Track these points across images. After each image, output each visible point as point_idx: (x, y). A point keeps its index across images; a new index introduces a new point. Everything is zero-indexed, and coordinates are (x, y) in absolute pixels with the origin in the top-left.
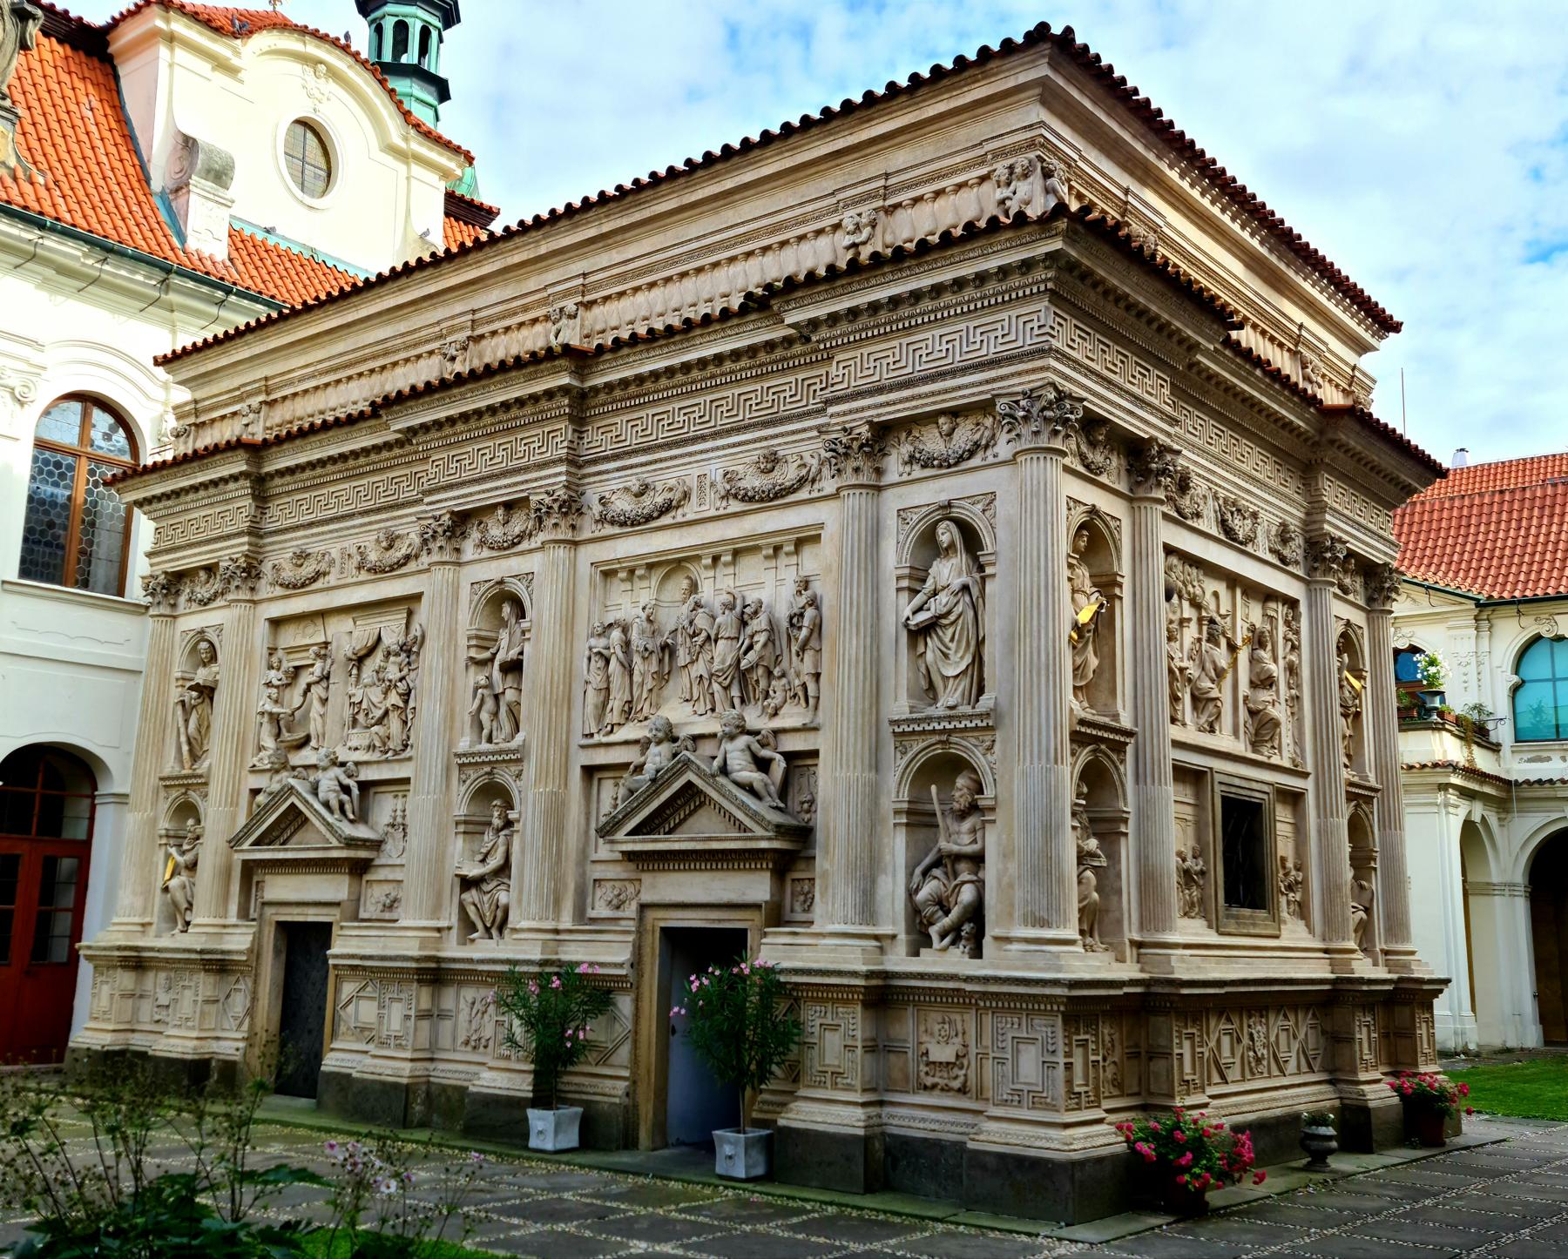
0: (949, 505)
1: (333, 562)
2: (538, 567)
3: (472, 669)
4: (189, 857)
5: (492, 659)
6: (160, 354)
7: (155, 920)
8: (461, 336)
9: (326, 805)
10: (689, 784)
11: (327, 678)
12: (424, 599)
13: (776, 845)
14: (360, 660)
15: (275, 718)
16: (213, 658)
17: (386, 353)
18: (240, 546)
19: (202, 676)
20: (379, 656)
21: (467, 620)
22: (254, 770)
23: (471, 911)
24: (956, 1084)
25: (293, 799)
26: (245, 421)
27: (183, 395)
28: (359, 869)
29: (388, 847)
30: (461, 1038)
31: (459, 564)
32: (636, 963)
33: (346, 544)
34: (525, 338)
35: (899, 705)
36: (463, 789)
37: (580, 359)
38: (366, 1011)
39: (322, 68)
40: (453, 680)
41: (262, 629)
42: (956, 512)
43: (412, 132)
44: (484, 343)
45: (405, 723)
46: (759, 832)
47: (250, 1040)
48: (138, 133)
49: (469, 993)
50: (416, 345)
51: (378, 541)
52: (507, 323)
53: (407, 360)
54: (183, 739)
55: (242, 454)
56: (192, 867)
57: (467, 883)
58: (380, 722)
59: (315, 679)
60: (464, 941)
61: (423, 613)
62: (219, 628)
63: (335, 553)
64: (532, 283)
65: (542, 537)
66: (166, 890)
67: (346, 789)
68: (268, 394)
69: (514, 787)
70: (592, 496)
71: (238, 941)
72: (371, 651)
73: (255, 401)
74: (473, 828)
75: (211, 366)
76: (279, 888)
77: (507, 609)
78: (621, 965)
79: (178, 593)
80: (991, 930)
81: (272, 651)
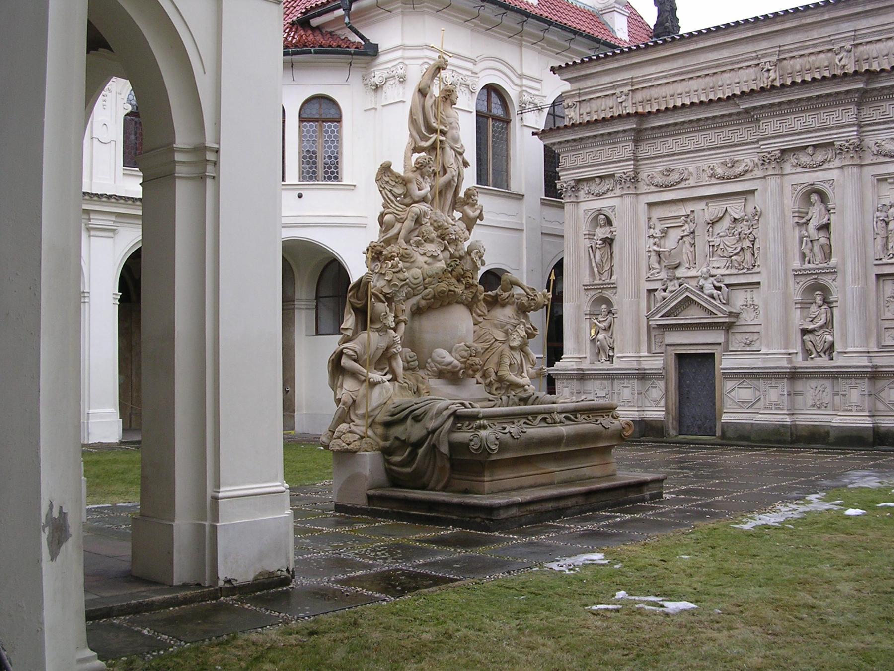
1: (691, 174)
2: (835, 177)
3: (797, 229)
4: (606, 324)
5: (807, 223)
6: (556, 64)
7: (588, 355)
8: (774, 59)
9: (712, 297)
11: (693, 232)
12: (756, 193)
14: (713, 223)
15: (658, 254)
16: (609, 222)
17: (718, 66)
18: (629, 166)
19: (602, 232)
20: (726, 223)
21: (791, 203)
22: (648, 280)
23: (809, 346)
25: (687, 294)
26: (620, 100)
27: (567, 87)
28: (728, 327)
29: (744, 315)
30: (810, 402)
31: (782, 175)
33: (699, 164)
36: (798, 287)
37: (871, 74)
38: (746, 394)
40: (784, 233)
41: (642, 207)
44: (785, 62)
45: (754, 255)
47: (667, 411)
49: (813, 383)
51: (724, 164)
52: (802, 52)
53: (731, 70)
54: (594, 265)
55: (635, 120)
56: (608, 328)
57: (805, 332)
58: (736, 255)
59: (686, 233)
60: (805, 359)
61: (757, 201)
62: (613, 208)
63: (691, 169)
64: (815, 34)
65: (837, 163)
66: (593, 341)
67: (718, 289)
68: (632, 86)
70: (870, 141)
71: (655, 364)
72: (721, 218)
73: (626, 90)
74: (804, 305)
75: (588, 72)
77: (814, 198)
79: (578, 190)
81: (649, 219)
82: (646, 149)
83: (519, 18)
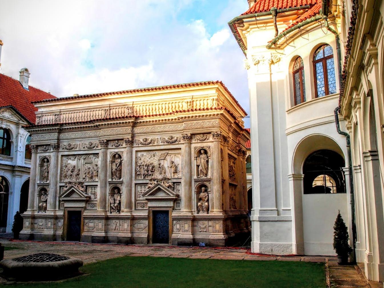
0: (203, 148)
10: (159, 188)
13: (175, 197)
24: (205, 231)
32: (148, 216)
35: (195, 177)
42: (203, 148)
46: (172, 195)
49: (114, 221)
69: (121, 188)
71: (60, 213)
76: (67, 205)
78: (146, 216)
80: (210, 210)
82: (62, 136)
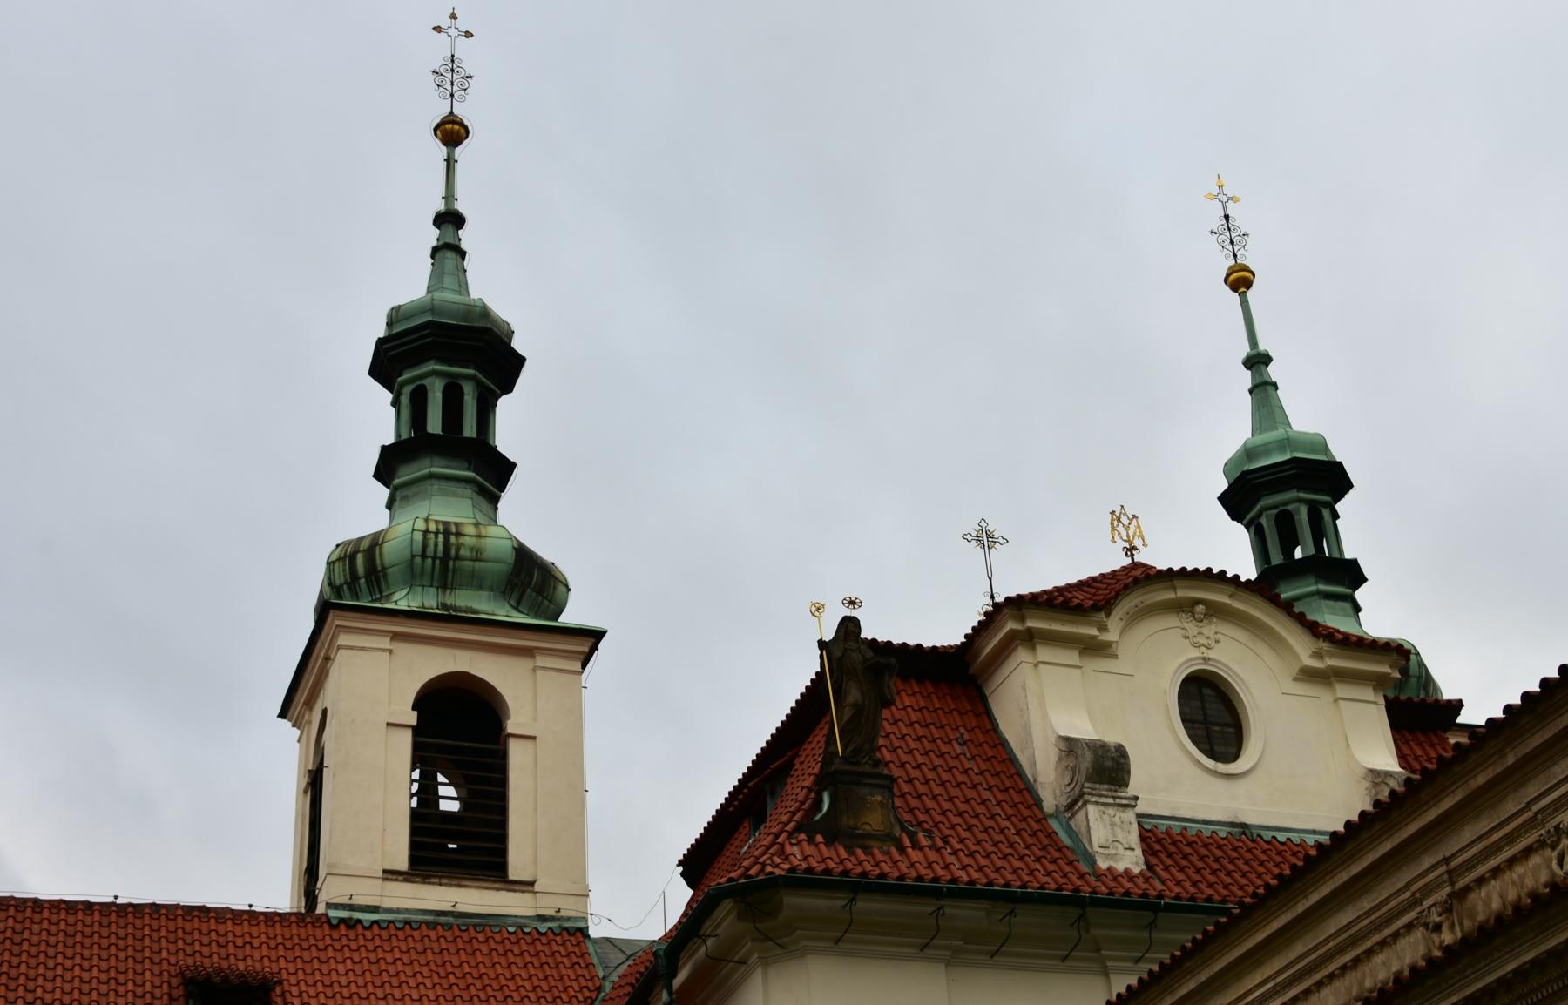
8: (1442, 895)
17: (1354, 941)
34: (1522, 877)
39: (1200, 608)
43: (1325, 645)
44: (1472, 896)
48: (1018, 753)
50: (1388, 921)
52: (1494, 862)
53: (1383, 944)
64: (1511, 807)
83: (1074, 912)
